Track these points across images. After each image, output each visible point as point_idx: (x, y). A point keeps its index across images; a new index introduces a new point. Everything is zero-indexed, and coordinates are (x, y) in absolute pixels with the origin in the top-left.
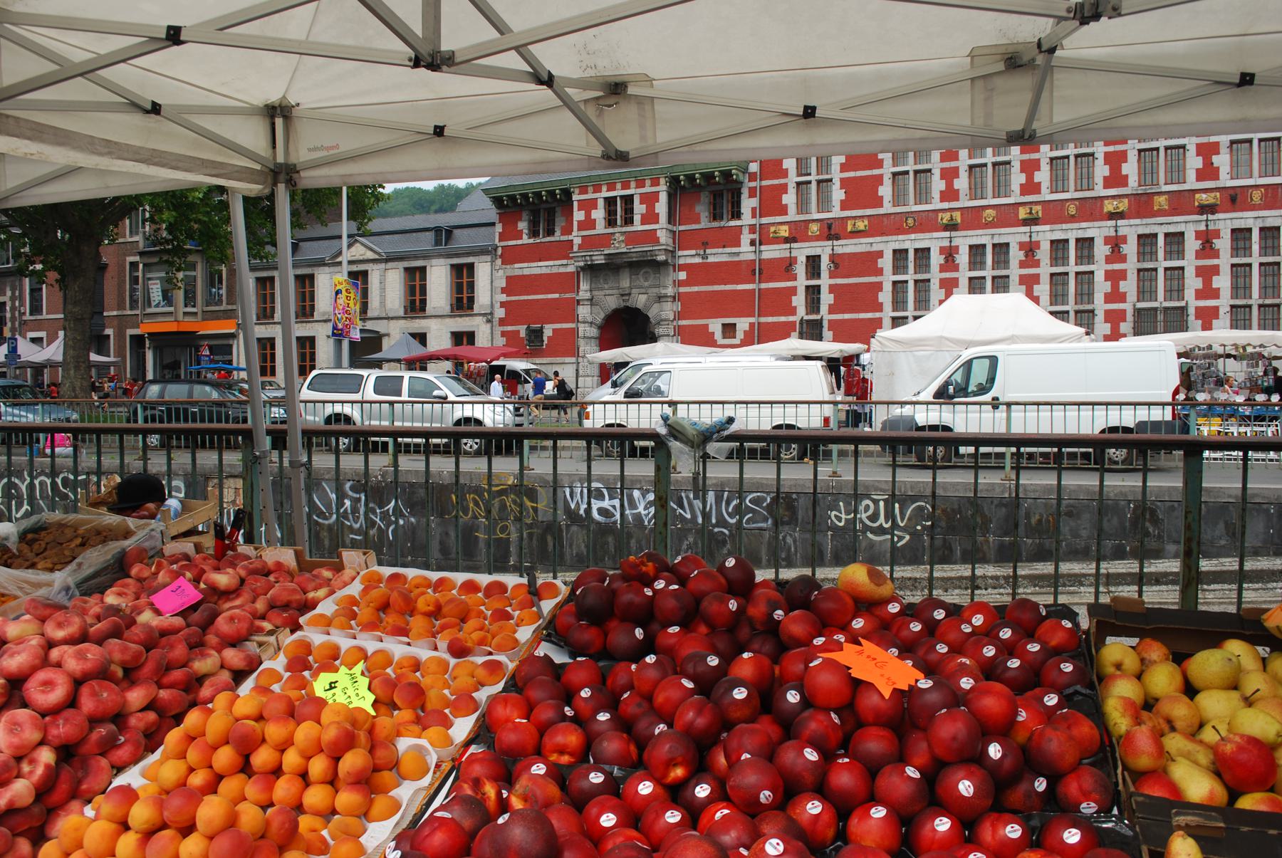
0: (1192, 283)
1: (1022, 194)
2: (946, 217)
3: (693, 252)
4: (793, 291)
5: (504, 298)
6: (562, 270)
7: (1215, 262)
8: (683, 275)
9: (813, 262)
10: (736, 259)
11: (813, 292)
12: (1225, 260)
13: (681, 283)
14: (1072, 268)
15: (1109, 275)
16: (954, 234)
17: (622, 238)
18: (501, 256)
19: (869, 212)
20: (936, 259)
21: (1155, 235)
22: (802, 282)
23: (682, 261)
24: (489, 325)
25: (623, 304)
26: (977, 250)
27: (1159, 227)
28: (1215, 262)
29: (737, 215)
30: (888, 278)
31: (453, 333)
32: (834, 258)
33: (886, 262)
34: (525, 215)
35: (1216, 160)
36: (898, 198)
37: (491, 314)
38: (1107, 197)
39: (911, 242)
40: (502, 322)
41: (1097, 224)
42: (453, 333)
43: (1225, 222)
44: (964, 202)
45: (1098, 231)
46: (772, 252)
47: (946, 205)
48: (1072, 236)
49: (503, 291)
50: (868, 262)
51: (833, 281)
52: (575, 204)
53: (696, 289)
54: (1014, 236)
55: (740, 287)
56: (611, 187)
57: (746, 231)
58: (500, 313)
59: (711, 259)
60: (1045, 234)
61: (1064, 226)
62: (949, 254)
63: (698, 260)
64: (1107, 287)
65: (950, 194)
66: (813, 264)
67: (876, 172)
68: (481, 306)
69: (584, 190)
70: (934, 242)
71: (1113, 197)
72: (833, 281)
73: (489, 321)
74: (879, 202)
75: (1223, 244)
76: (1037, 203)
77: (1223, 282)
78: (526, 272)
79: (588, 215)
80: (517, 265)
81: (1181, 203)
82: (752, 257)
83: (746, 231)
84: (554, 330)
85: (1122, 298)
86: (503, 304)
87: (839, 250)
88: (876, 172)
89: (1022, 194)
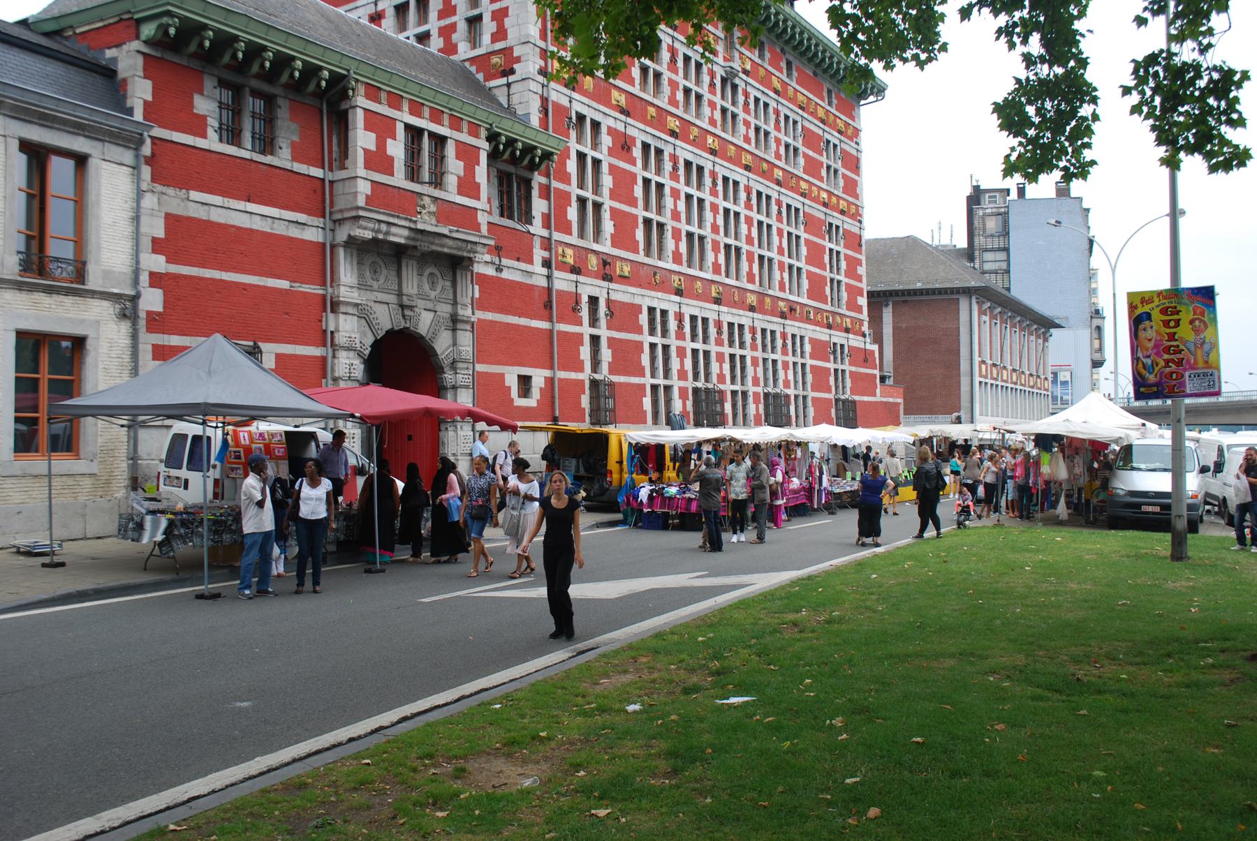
5: (159, 263)
6: (294, 232)
10: (529, 281)
17: (433, 208)
18: (150, 161)
24: (125, 327)
25: (403, 325)
29: (527, 218)
31: (21, 335)
32: (608, 301)
34: (209, 83)
37: (135, 299)
40: (156, 323)
42: (21, 335)
46: (563, 281)
49: (158, 246)
52: (360, 114)
55: (523, 321)
56: (416, 109)
57: (537, 243)
58: (152, 300)
59: (505, 275)
63: (490, 271)
68: (107, 274)
69: (373, 93)
73: (123, 316)
78: (217, 216)
79: (381, 145)
80: (194, 195)
82: (543, 283)
83: (537, 243)
84: (279, 357)
86: (157, 279)
87: (614, 296)
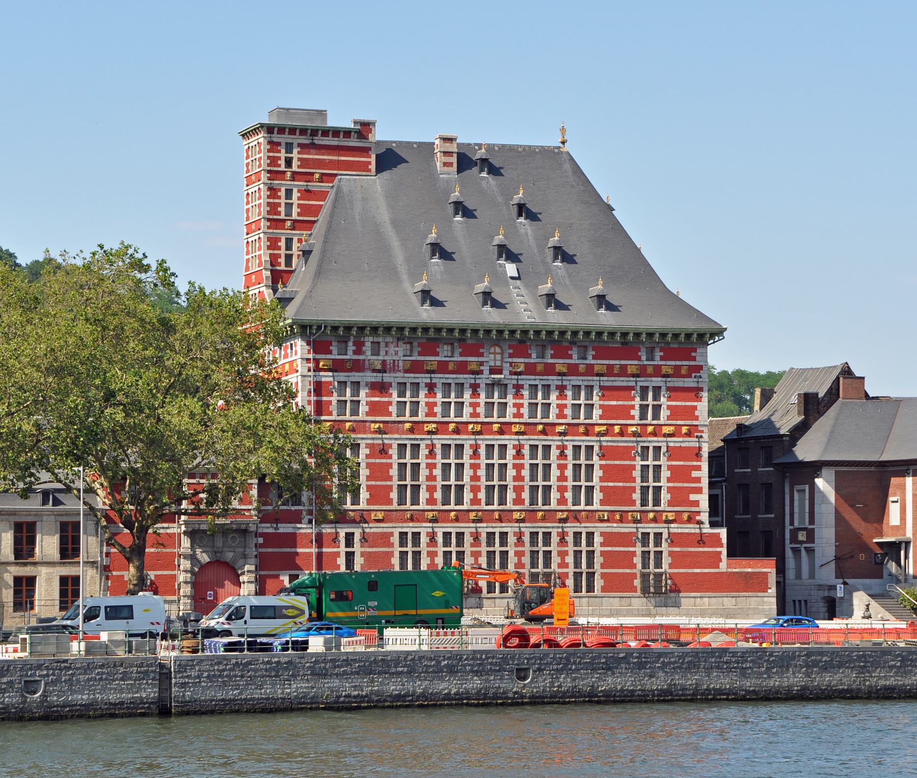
0: (555, 560)
1: (471, 505)
2: (430, 515)
3: (269, 525)
4: (338, 554)
7: (566, 549)
8: (261, 540)
9: (349, 538)
11: (350, 556)
12: (571, 548)
13: (261, 546)
14: (497, 548)
15: (517, 554)
16: (435, 525)
19: (385, 507)
20: (424, 539)
21: (538, 533)
22: (343, 549)
23: (260, 531)
26: (447, 535)
27: (541, 528)
28: (566, 549)
30: (397, 550)
33: (395, 539)
35: (566, 494)
36: (402, 501)
38: (515, 511)
39: (410, 528)
41: (510, 525)
43: (571, 528)
44: (440, 507)
45: (510, 529)
47: (429, 507)
48: (497, 531)
50: (385, 539)
51: (363, 550)
53: (270, 550)
54: (468, 529)
60: (484, 529)
61: (494, 525)
62: (432, 537)
63: (271, 530)
64: (516, 560)
65: (431, 501)
66: (349, 538)
67: (388, 483)
70: (424, 529)
71: (518, 511)
72: (363, 550)
74: (390, 502)
75: (570, 539)
76: (479, 511)
77: (570, 559)
81: (549, 516)
85: (523, 566)
88: (388, 483)
89: (471, 505)
